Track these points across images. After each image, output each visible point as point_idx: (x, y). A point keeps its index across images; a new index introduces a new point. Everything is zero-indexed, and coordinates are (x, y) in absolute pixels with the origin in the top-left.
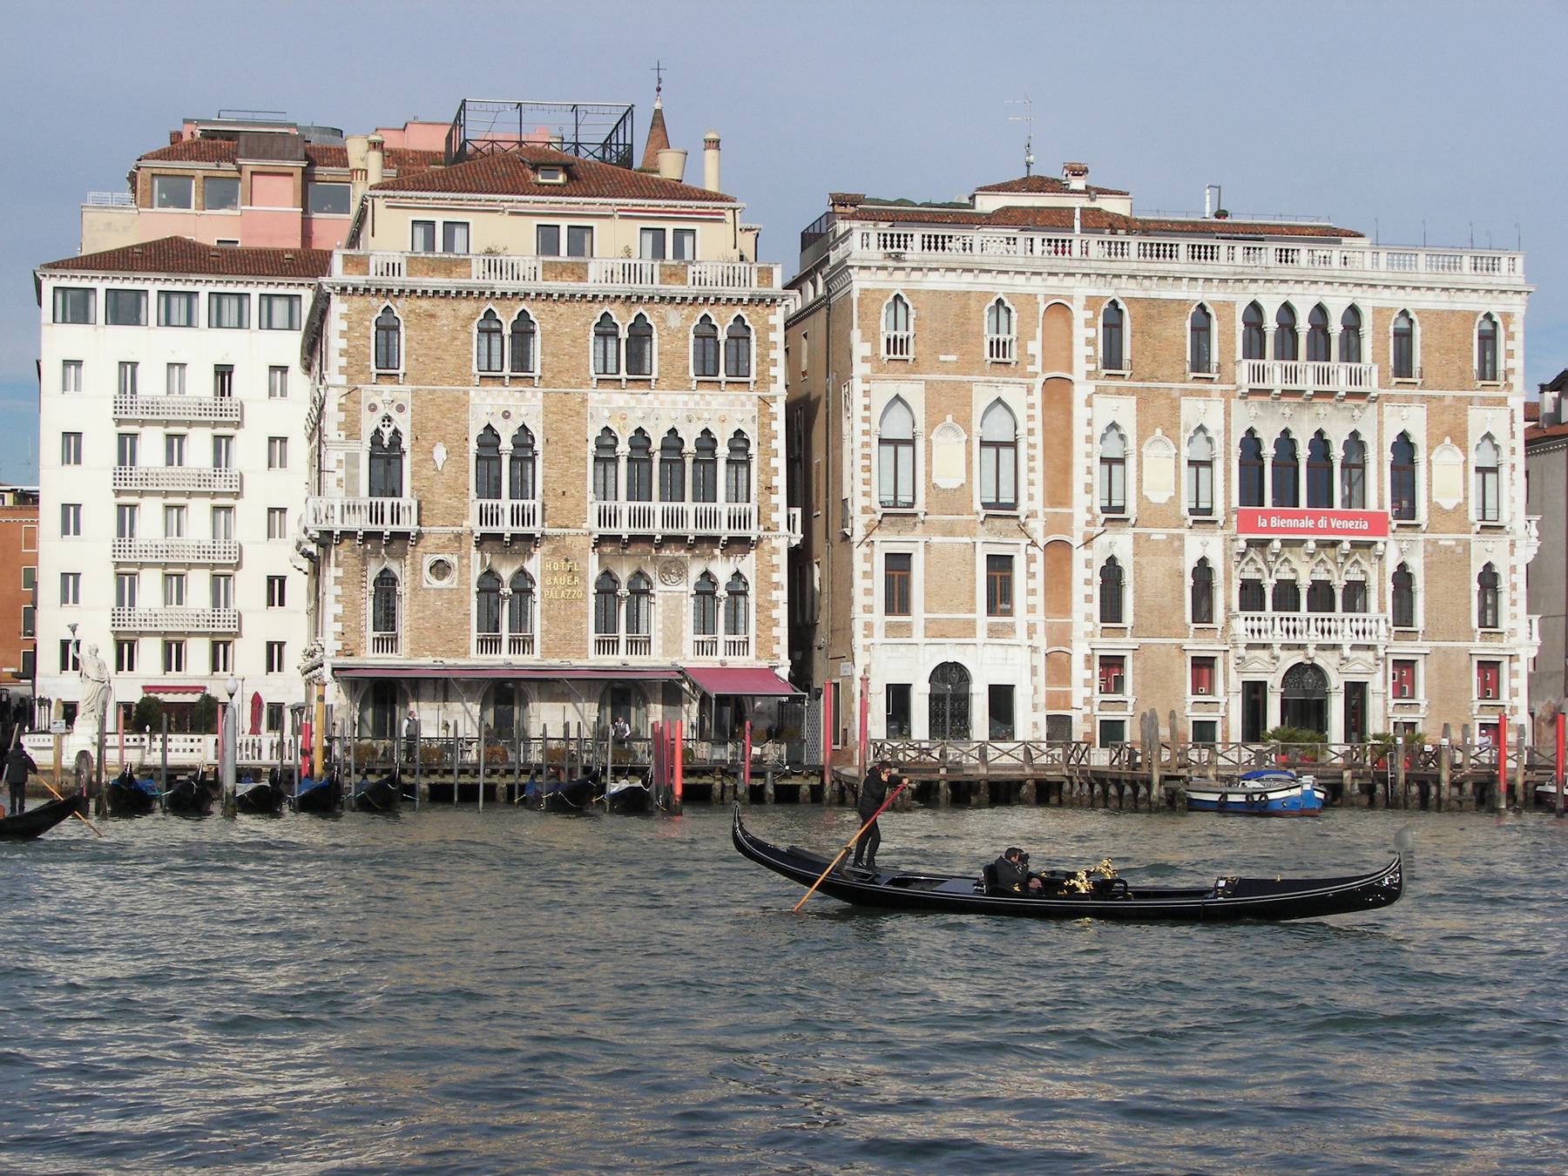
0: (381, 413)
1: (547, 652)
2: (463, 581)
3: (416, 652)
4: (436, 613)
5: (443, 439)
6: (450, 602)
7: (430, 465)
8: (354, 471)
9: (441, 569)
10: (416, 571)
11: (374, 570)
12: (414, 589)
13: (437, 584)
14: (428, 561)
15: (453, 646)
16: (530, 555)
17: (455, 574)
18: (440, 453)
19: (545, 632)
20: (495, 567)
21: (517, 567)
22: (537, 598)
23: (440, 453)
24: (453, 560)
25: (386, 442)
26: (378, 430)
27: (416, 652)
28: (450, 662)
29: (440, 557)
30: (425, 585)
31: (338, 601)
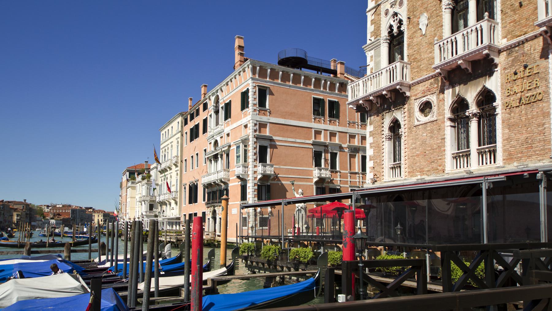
0: (391, 11)
1: (509, 158)
2: (441, 113)
3: (411, 173)
4: (424, 143)
5: (426, 10)
6: (432, 132)
7: (418, 34)
8: (378, 60)
9: (426, 107)
10: (411, 114)
11: (387, 120)
12: (409, 128)
13: (423, 119)
14: (416, 105)
15: (434, 165)
16: (491, 74)
17: (435, 109)
18: (423, 20)
19: (508, 140)
20: (462, 94)
21: (479, 89)
22: (499, 111)
23: (423, 20)
24: (433, 99)
25: (395, 30)
26: (391, 27)
27: (411, 173)
28: (427, 178)
29: (424, 99)
30: (416, 123)
31: (371, 147)
